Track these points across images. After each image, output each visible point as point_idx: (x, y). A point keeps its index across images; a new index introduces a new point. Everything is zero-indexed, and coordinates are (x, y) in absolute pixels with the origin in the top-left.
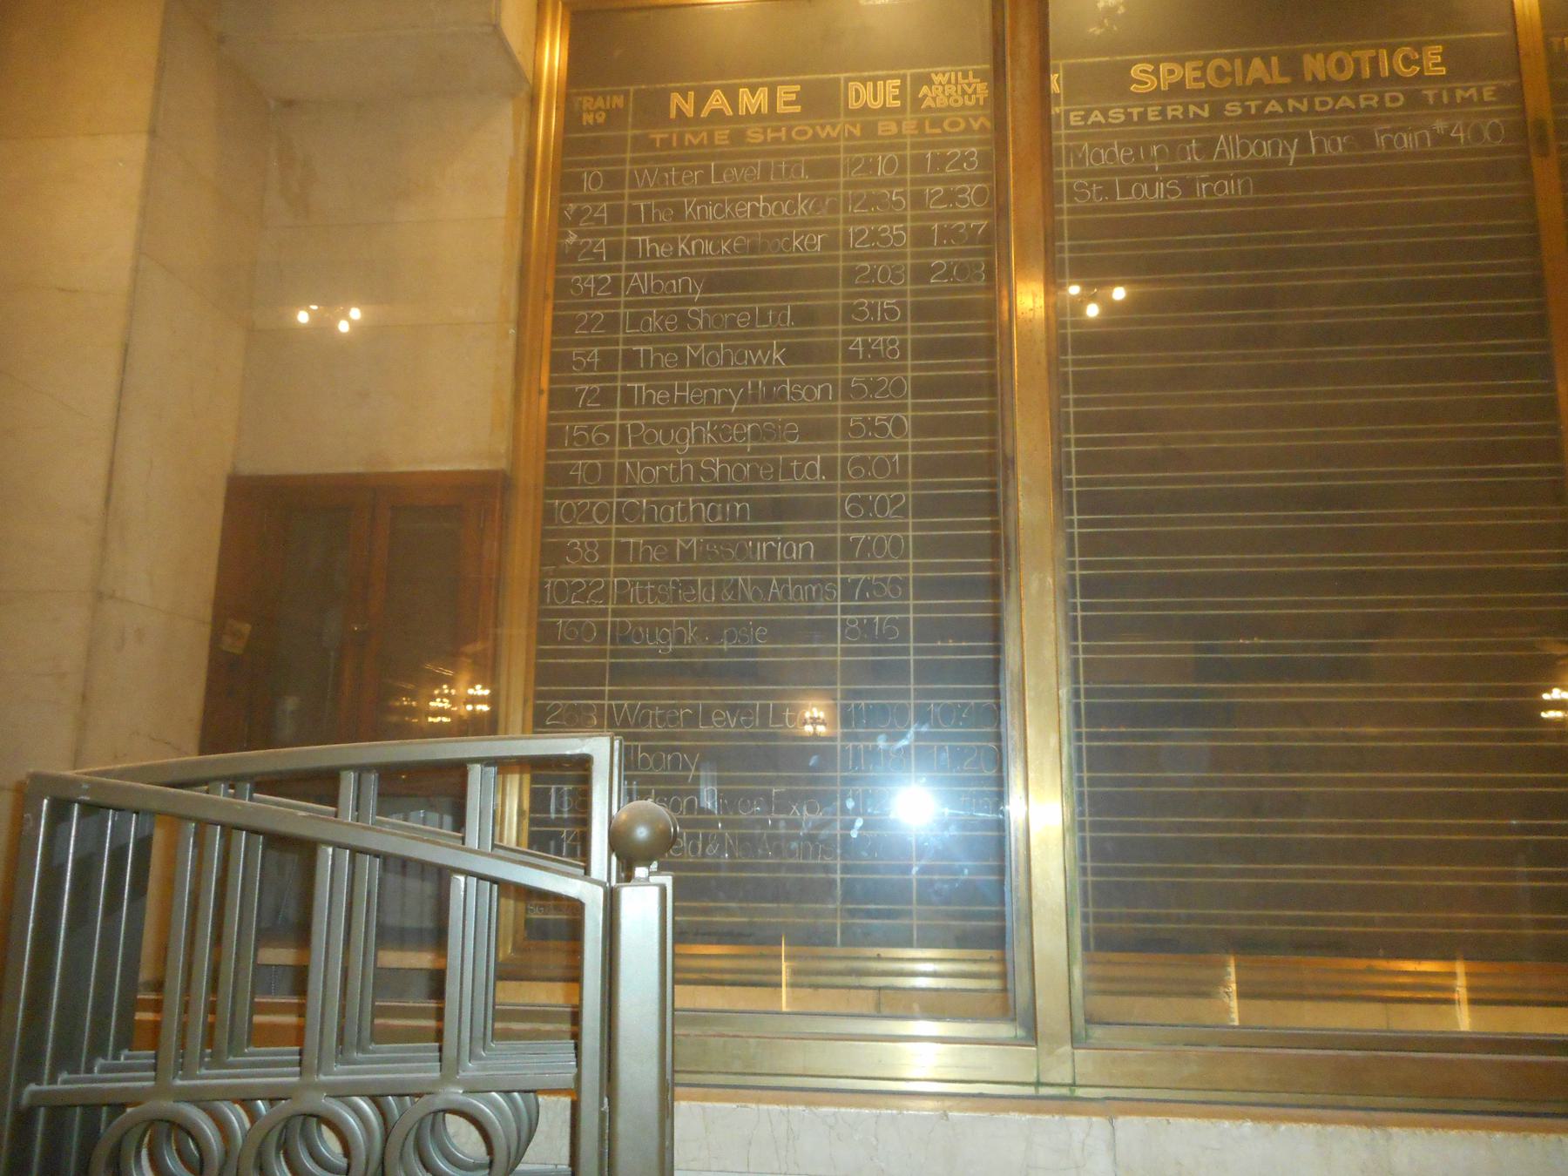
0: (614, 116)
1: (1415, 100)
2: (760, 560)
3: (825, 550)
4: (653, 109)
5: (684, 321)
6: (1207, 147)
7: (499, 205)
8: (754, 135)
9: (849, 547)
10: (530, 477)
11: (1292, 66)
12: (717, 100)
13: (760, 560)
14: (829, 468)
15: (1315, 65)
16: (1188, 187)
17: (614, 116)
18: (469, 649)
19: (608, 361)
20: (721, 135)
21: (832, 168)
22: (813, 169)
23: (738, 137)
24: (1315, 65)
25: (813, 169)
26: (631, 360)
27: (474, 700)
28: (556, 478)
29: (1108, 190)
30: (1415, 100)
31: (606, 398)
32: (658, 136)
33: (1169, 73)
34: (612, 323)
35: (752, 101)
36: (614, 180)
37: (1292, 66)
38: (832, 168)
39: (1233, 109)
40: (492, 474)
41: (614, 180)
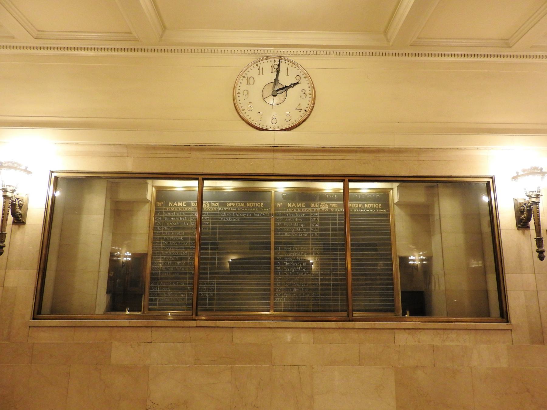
0: (162, 205)
1: (259, 210)
2: (179, 264)
3: (187, 263)
4: (167, 204)
5: (170, 233)
6: (235, 214)
7: (147, 218)
8: (180, 209)
9: (189, 263)
10: (150, 253)
11: (246, 204)
12: (175, 204)
13: (179, 264)
14: (187, 253)
15: (248, 204)
16: (233, 219)
17: (162, 205)
18: (126, 242)
19: (160, 238)
20: (176, 209)
21: (189, 214)
22: (187, 214)
23: (178, 209)
24: (248, 204)
25: (187, 214)
26: (163, 238)
27: (126, 256)
28: (153, 254)
29: (223, 219)
30: (259, 210)
31: (160, 243)
32: (168, 208)
33: (232, 204)
34: (161, 233)
35: (180, 204)
36: (162, 214)
37: (246, 204)
38: (189, 214)
39: (239, 209)
40: (144, 254)
41: (162, 214)
